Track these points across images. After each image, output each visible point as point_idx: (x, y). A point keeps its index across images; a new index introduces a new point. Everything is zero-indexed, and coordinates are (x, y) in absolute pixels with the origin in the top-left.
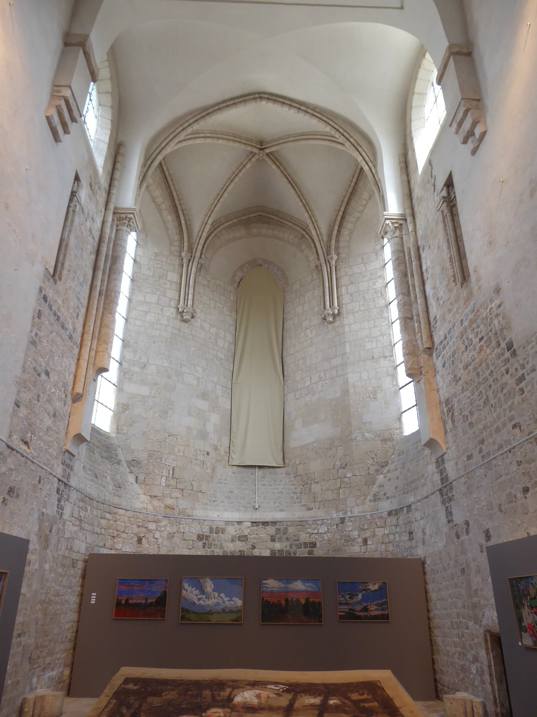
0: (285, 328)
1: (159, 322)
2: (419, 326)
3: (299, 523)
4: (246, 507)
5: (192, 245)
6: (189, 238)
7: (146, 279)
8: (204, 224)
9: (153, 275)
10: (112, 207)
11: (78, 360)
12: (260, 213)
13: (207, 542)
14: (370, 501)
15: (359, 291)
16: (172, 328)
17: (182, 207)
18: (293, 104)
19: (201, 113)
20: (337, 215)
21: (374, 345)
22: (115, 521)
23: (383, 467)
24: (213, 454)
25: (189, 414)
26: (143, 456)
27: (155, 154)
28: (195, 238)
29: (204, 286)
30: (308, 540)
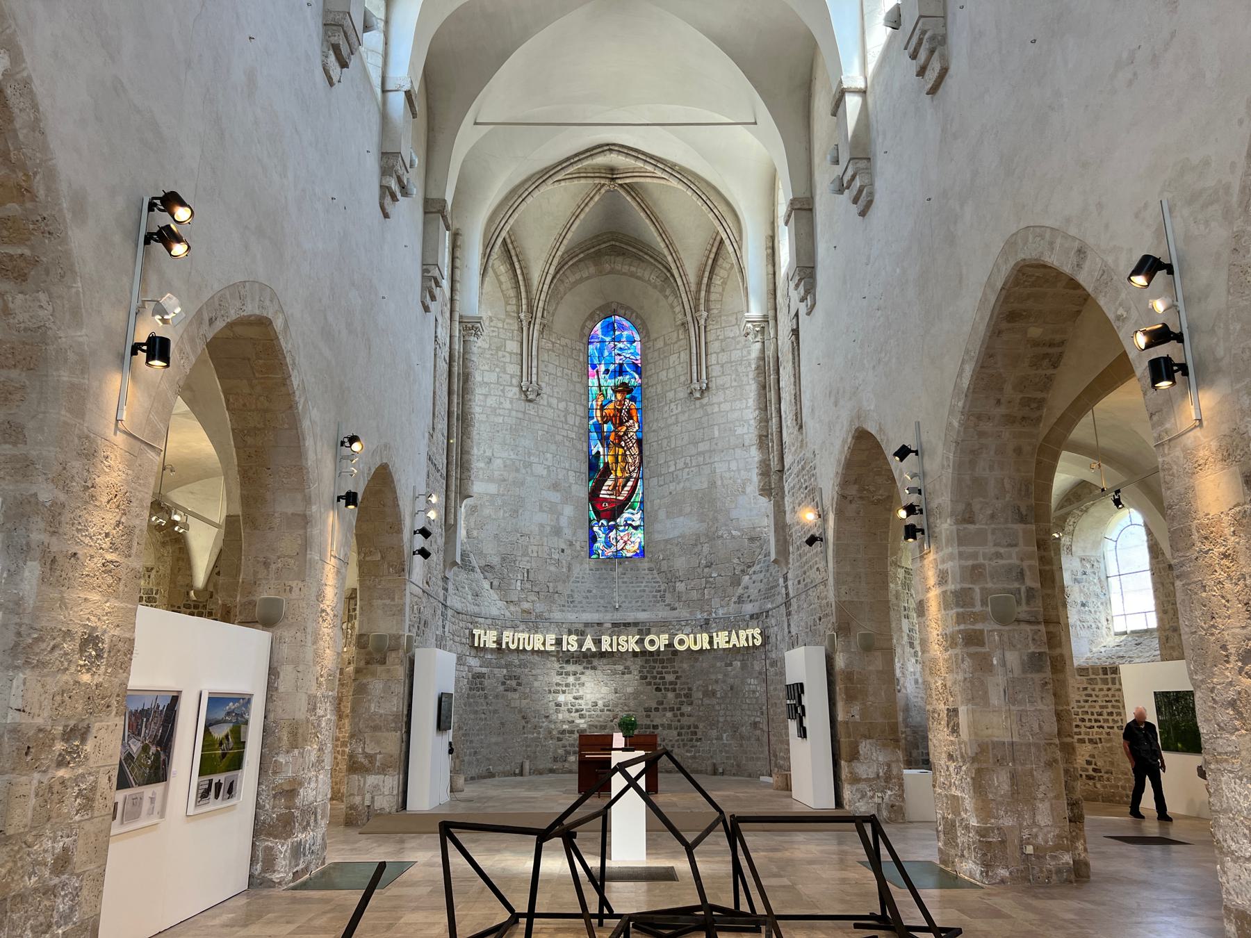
2: (773, 447)
6: (527, 292)
8: (545, 274)
10: (457, 317)
11: (446, 491)
14: (735, 603)
21: (745, 430)
23: (749, 567)
24: (568, 552)
25: (541, 510)
26: (495, 560)
27: (494, 237)
28: (535, 292)
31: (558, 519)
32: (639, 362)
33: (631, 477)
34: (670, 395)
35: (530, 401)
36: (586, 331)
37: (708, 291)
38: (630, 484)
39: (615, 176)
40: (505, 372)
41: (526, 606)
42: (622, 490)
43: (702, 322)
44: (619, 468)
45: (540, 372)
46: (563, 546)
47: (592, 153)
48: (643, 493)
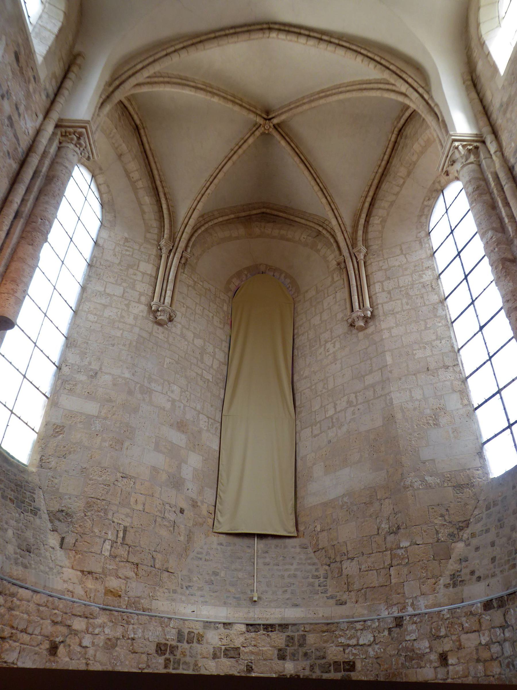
0: (296, 346)
3: (325, 628)
4: (238, 599)
5: (174, 234)
6: (171, 226)
7: (109, 267)
9: (120, 263)
10: (55, 116)
12: (264, 210)
13: (172, 658)
14: (446, 586)
15: (399, 287)
16: (141, 329)
18: (312, 34)
20: (364, 203)
21: (428, 352)
22: (11, 609)
23: (461, 529)
25: (157, 448)
29: (188, 286)
30: (340, 658)
31: (179, 467)
40: (133, 288)
41: (113, 583)
46: (184, 505)
47: (249, 28)
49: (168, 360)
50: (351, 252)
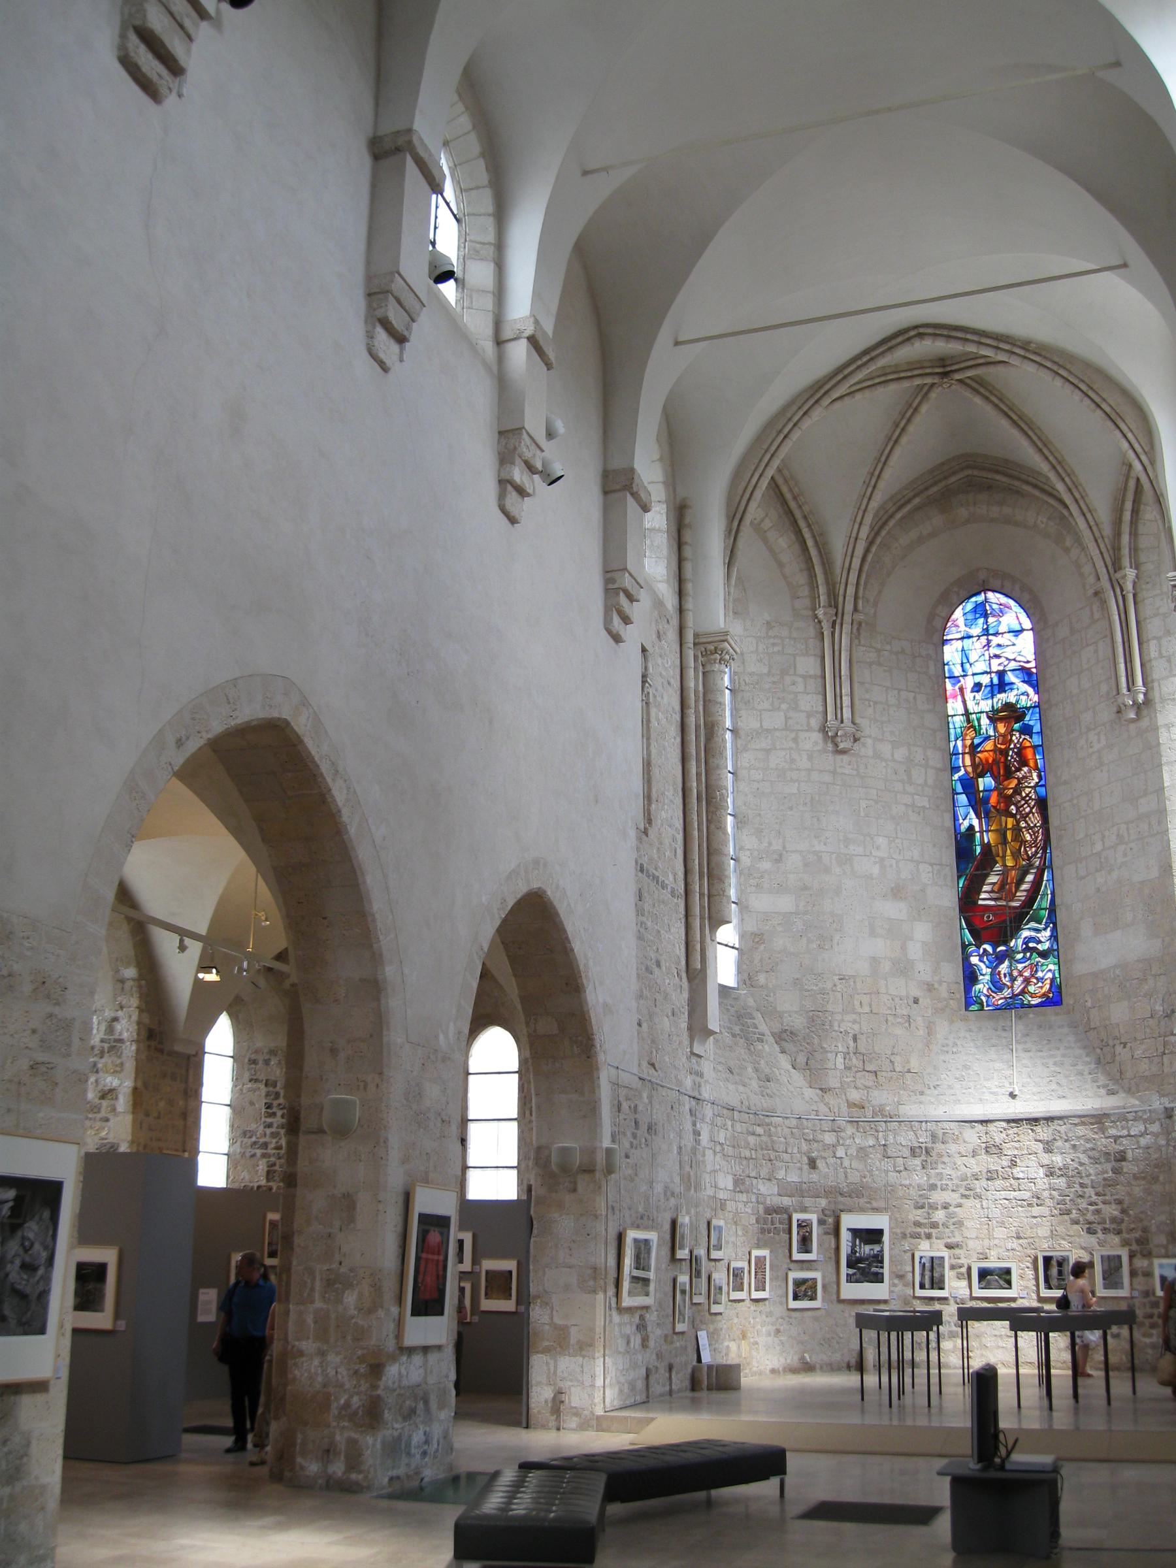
1: (794, 766)
5: (834, 588)
6: (825, 573)
7: (757, 684)
8: (852, 540)
9: (769, 671)
10: (689, 637)
17: (802, 511)
18: (984, 340)
19: (812, 396)
25: (873, 933)
26: (798, 1022)
29: (870, 664)
31: (904, 948)
32: (1032, 664)
33: (1031, 866)
34: (1087, 717)
35: (844, 752)
36: (938, 623)
37: (1134, 534)
38: (1030, 878)
39: (948, 369)
40: (796, 708)
41: (855, 1096)
42: (1017, 889)
43: (1129, 586)
44: (1008, 851)
45: (857, 702)
46: (915, 992)
48: (1053, 893)
49: (863, 804)
50: (1113, 579)
